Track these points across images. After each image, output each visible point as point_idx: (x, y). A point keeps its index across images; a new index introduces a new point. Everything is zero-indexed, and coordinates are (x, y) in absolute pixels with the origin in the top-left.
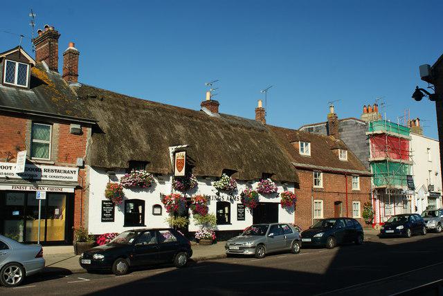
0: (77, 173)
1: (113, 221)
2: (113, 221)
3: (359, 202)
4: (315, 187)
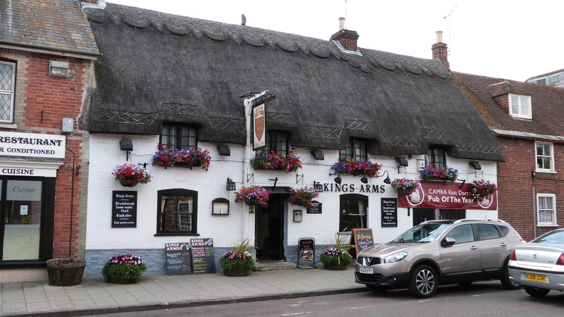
0: (63, 144)
1: (134, 226)
2: (134, 226)
3: (553, 196)
4: (538, 170)
